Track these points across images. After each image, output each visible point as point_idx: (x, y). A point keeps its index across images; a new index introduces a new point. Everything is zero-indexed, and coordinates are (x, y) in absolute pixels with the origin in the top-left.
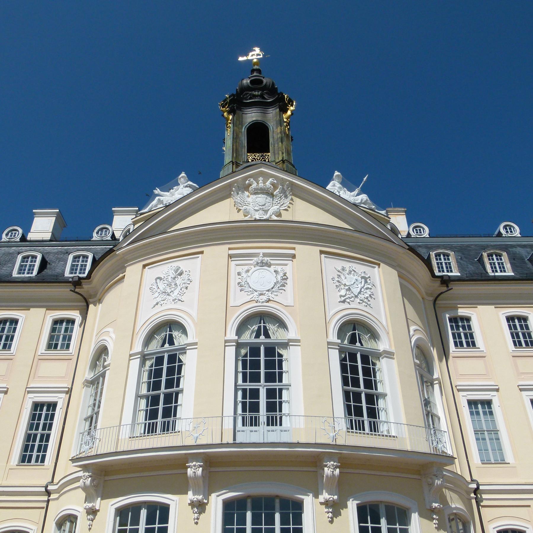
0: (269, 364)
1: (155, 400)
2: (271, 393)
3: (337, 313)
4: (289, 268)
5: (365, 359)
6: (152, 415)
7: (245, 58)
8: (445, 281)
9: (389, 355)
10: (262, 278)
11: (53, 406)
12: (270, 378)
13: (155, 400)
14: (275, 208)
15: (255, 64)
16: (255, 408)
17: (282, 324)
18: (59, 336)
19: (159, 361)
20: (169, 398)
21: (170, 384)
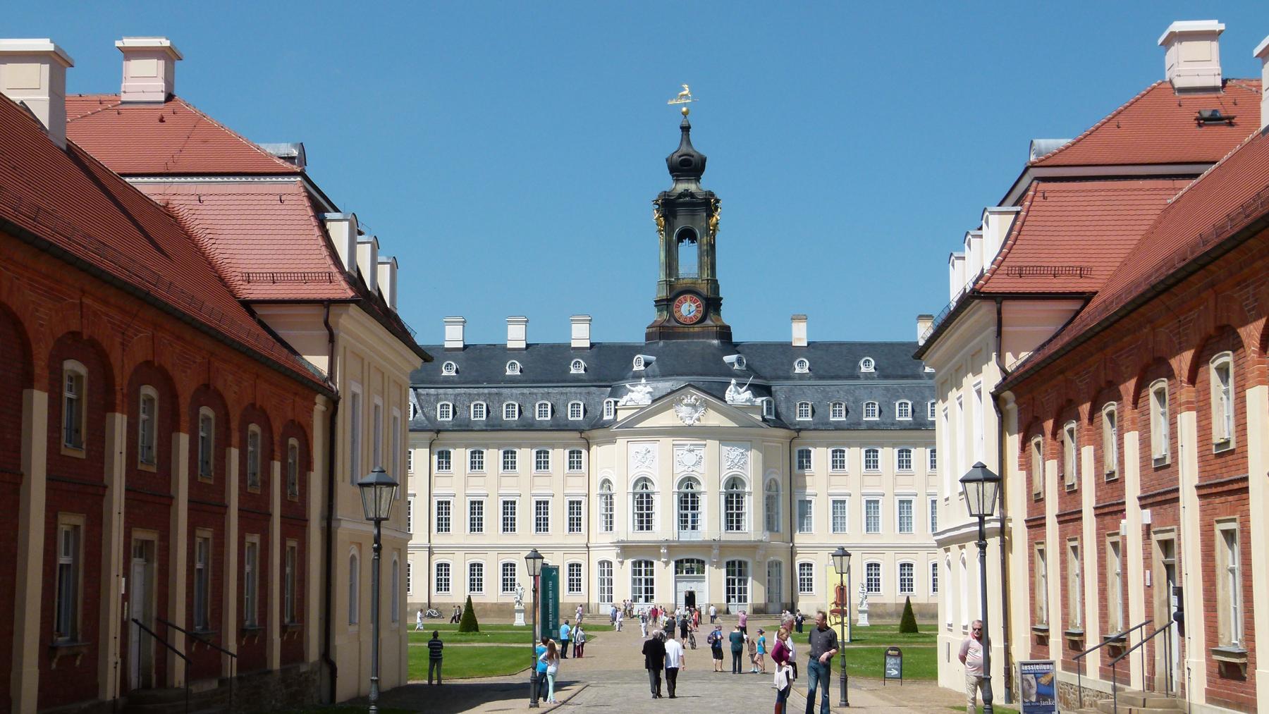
0: (693, 502)
1: (642, 515)
2: (693, 516)
3: (726, 474)
4: (702, 452)
5: (738, 496)
6: (642, 522)
7: (674, 102)
8: (800, 429)
9: (750, 493)
10: (690, 458)
11: (579, 503)
12: (693, 508)
13: (642, 515)
14: (696, 415)
15: (685, 114)
16: (686, 522)
17: (699, 483)
18: (574, 463)
19: (642, 496)
20: (648, 515)
21: (648, 509)
